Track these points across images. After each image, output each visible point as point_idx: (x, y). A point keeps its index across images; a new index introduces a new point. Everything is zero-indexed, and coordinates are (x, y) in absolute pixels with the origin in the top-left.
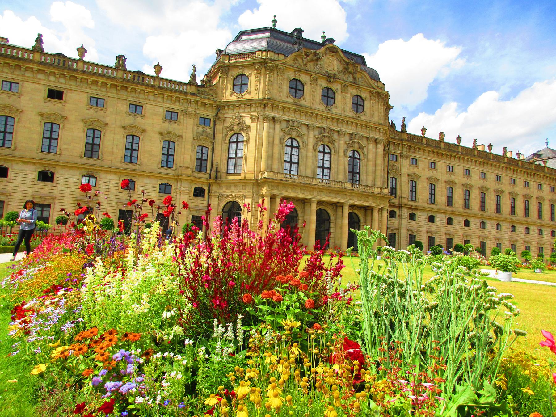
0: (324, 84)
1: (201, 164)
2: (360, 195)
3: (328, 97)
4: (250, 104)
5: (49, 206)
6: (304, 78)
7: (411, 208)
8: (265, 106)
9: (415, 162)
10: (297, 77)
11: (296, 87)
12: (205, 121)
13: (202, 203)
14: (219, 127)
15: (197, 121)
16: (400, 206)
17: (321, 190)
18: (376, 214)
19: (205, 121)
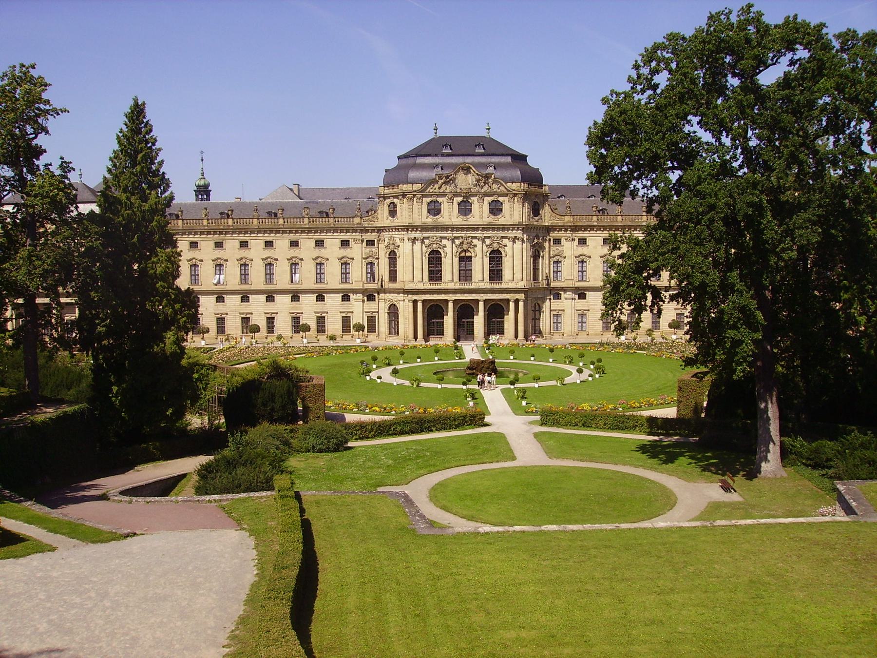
0: (460, 199)
1: (372, 276)
2: (493, 291)
3: (465, 208)
4: (397, 229)
5: (273, 318)
6: (440, 199)
7: (577, 288)
8: (408, 230)
9: (582, 242)
10: (434, 199)
11: (435, 209)
12: (370, 243)
13: (371, 306)
14: (382, 246)
15: (364, 244)
16: (565, 290)
17: (455, 291)
18: (512, 305)
19: (370, 243)
